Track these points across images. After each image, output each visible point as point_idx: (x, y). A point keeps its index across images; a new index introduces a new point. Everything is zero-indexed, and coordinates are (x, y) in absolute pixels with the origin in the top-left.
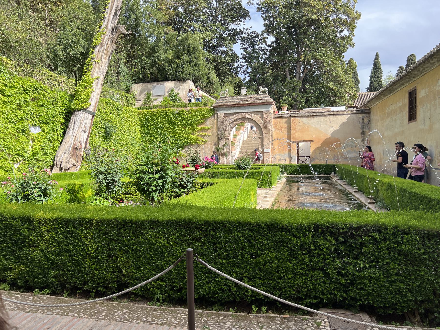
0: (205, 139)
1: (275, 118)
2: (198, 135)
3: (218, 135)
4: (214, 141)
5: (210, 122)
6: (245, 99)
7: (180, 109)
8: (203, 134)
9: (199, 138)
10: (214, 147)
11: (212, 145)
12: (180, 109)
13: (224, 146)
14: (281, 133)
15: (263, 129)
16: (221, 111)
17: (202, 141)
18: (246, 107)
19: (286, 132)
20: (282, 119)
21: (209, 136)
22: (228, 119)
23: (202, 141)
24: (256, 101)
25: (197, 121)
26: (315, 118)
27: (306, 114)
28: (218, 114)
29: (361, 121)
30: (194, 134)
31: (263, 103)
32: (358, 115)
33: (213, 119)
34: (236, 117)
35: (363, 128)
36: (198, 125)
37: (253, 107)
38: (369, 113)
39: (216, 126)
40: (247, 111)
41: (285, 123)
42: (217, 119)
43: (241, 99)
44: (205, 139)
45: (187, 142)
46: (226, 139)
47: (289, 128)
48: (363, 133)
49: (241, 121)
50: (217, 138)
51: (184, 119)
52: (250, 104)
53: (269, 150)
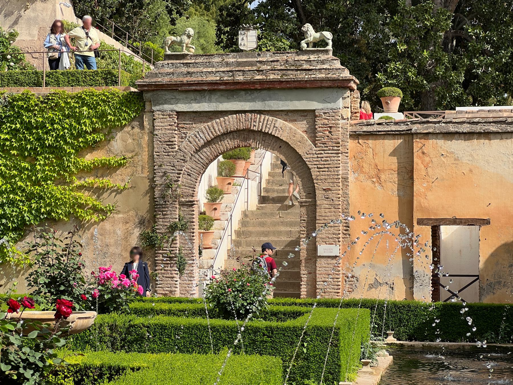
0: (107, 201)
1: (355, 136)
2: (80, 188)
3: (152, 188)
4: (136, 209)
5: (124, 141)
6: (251, 64)
7: (18, 91)
8: (98, 182)
9: (84, 196)
10: (137, 232)
11: (130, 226)
12: (18, 91)
13: (173, 228)
14: (378, 187)
15: (314, 173)
16: (166, 102)
17: (95, 210)
18: (256, 94)
19: (395, 187)
21: (118, 191)
22: (190, 133)
23: (95, 210)
24: (292, 76)
25: (76, 138)
26: (496, 143)
27: (466, 128)
28: (157, 115)
30: (65, 183)
31: (315, 81)
33: (137, 130)
34: (218, 126)
36: (79, 151)
37: (280, 94)
39: (145, 156)
40: (258, 105)
41: (393, 154)
42: (152, 133)
43: (239, 64)
44: (107, 201)
45: (38, 210)
46: (182, 204)
47: (407, 175)
49: (236, 142)
50: (147, 198)
51: (29, 127)
52: (272, 82)
53: (335, 250)
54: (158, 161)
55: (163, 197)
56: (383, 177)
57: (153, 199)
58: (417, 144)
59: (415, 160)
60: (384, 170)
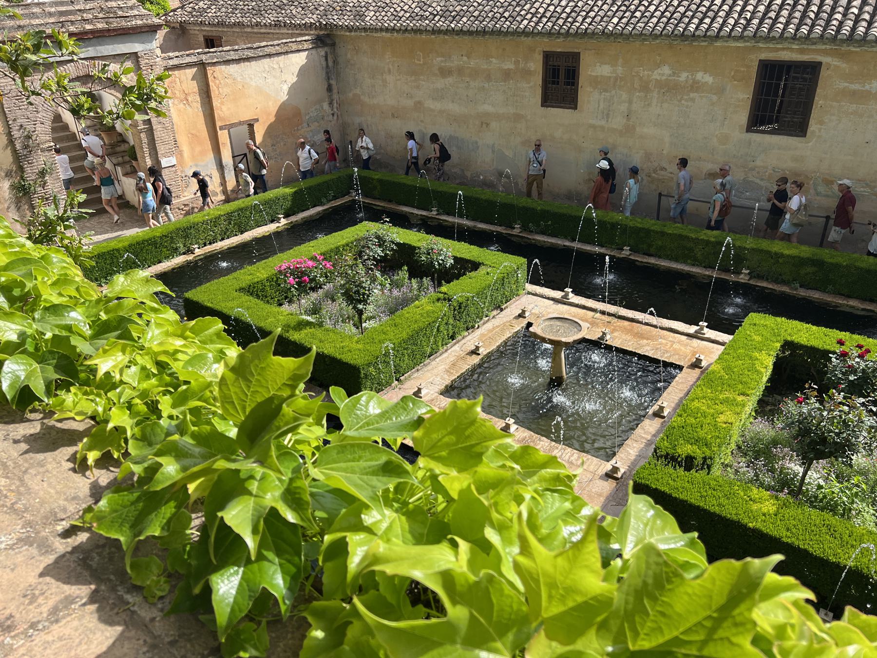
3: (11, 141)
10: (6, 184)
13: (42, 173)
20: (182, 71)
29: (324, 63)
32: (319, 50)
35: (329, 79)
38: (333, 45)
41: (193, 79)
43: (62, 13)
48: (329, 89)
50: (9, 151)
53: (173, 161)
54: (10, 117)
55: (26, 147)
56: (190, 99)
57: (15, 151)
58: (210, 70)
59: (211, 84)
60: (189, 94)
